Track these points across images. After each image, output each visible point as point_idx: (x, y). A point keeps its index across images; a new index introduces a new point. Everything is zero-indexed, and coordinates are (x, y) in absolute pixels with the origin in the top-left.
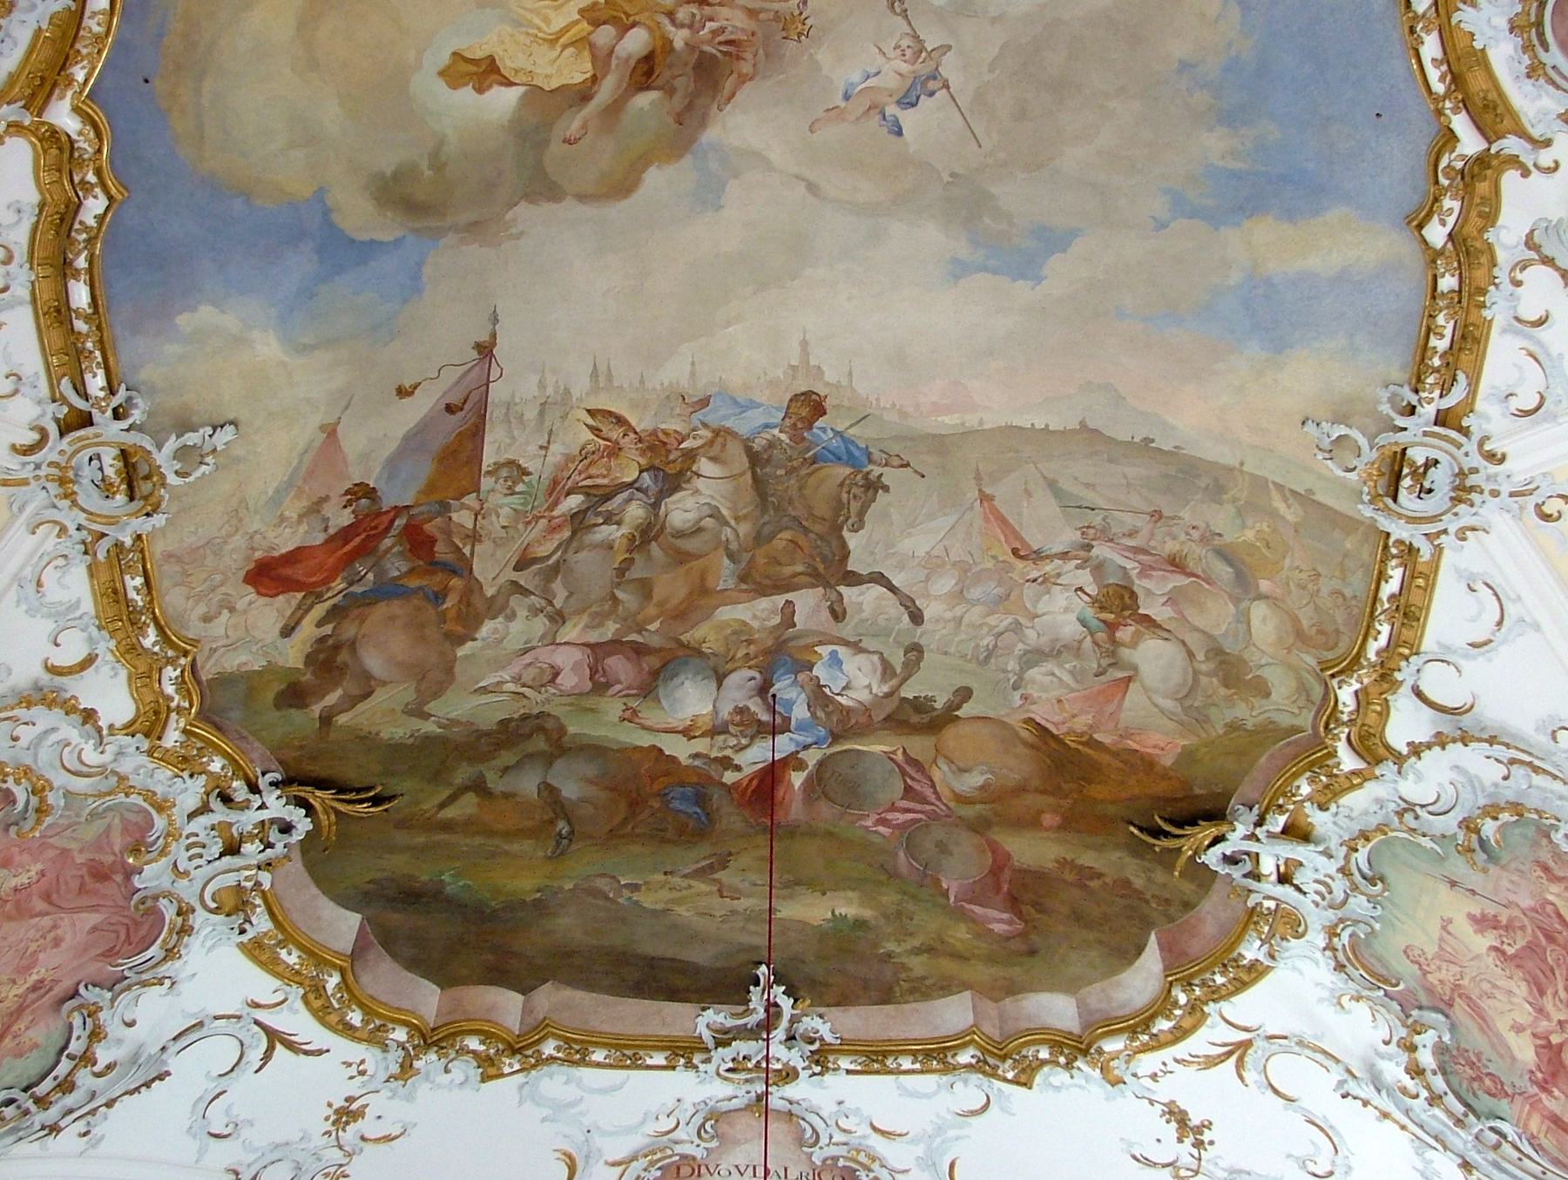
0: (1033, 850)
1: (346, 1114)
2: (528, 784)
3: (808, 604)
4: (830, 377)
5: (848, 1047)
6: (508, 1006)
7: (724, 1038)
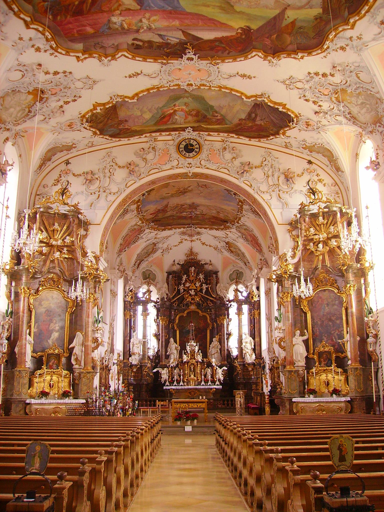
0: (212, 220)
4: (195, 202)
5: (198, 227)
6: (170, 227)
7: (188, 227)
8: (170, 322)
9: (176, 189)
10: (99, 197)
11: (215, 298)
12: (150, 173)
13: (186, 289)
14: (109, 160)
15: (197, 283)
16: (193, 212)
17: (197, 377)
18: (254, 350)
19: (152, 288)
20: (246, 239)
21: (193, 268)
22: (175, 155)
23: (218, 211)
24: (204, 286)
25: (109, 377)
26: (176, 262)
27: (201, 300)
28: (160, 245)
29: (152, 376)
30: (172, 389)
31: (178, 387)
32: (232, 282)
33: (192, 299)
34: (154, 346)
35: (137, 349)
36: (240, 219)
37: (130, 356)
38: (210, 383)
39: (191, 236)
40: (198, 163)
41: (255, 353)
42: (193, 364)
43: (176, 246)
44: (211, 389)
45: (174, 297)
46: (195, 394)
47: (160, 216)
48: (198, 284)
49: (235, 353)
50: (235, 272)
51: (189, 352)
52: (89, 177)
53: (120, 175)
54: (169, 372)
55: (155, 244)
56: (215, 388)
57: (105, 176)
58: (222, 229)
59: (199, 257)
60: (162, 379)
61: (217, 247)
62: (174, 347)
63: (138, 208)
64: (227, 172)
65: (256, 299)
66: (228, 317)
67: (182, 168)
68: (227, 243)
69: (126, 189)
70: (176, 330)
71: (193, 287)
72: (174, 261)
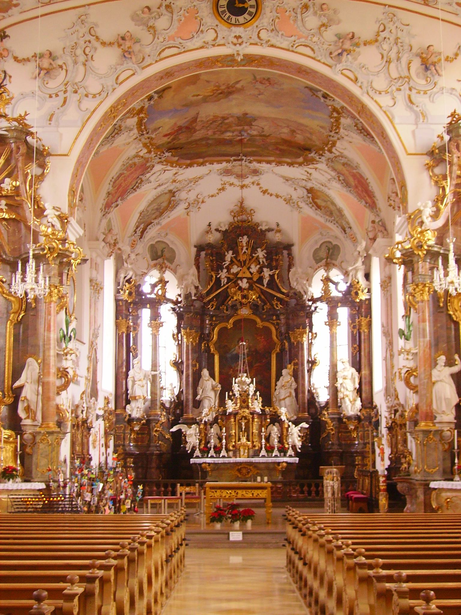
1: (176, 173)
2: (204, 142)
3: (246, 127)
5: (254, 160)
6: (201, 160)
7: (235, 160)
8: (201, 339)
9: (211, 87)
10: (65, 102)
11: (287, 295)
12: (164, 55)
13: (231, 277)
14: (84, 30)
15: (253, 266)
16: (246, 131)
17: (253, 442)
18: (359, 391)
19: (168, 276)
20: (346, 184)
21: (245, 237)
22: (210, 20)
23: (293, 128)
24: (267, 273)
25: (88, 441)
26: (213, 227)
27: (259, 297)
28: (183, 195)
29: (168, 439)
30: (205, 463)
31: (217, 460)
32: (319, 264)
33: (244, 297)
34: (171, 384)
35: (140, 390)
36: (334, 144)
37: (128, 402)
38: (276, 452)
39: (241, 176)
40: (255, 36)
41: (361, 397)
42: (245, 418)
43: (212, 196)
44: (279, 463)
45: (209, 293)
46: (248, 473)
47: (183, 138)
48: (254, 269)
49: (323, 396)
50: (325, 244)
51: (237, 395)
52: (45, 63)
53: (106, 59)
54: (200, 432)
55: (172, 193)
56: (286, 462)
57: (75, 63)
58: (300, 164)
59: (258, 218)
60: (188, 446)
61: (291, 198)
62: (209, 386)
63: (140, 123)
64: (311, 53)
65: (363, 296)
66: (311, 331)
67: (224, 45)
68: (310, 191)
69: (116, 86)
70: (213, 355)
71: (244, 273)
72: (209, 225)
